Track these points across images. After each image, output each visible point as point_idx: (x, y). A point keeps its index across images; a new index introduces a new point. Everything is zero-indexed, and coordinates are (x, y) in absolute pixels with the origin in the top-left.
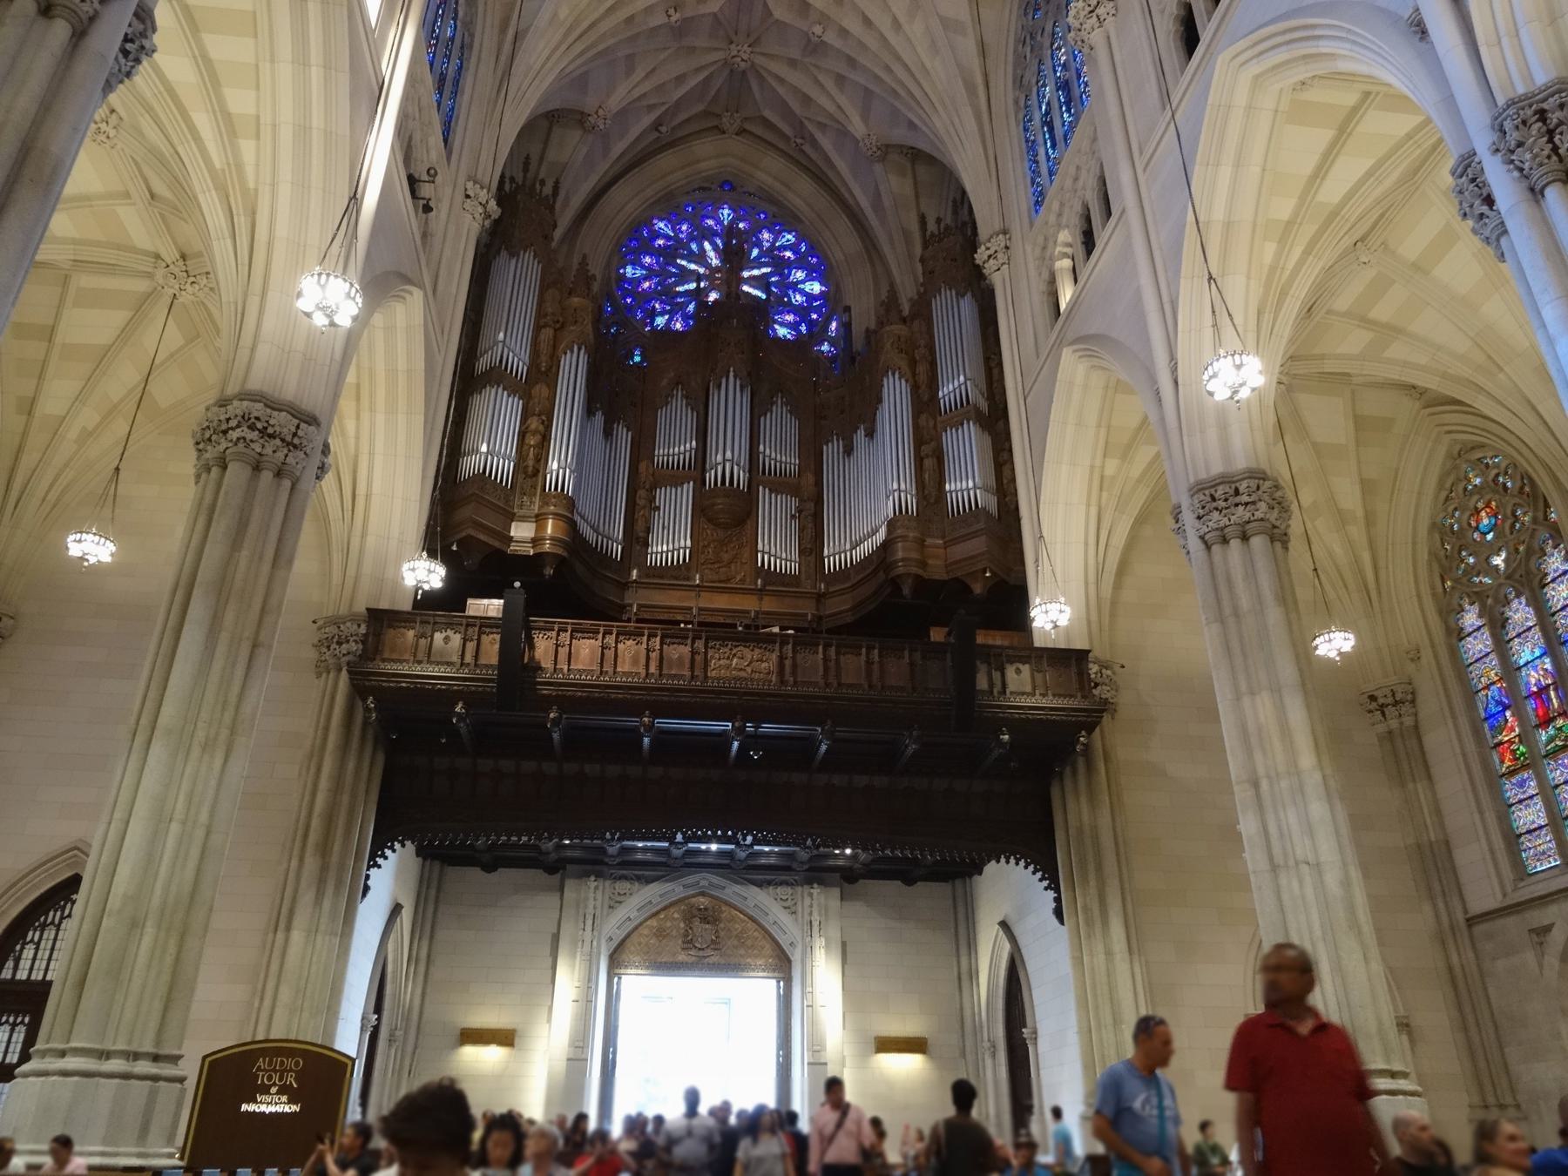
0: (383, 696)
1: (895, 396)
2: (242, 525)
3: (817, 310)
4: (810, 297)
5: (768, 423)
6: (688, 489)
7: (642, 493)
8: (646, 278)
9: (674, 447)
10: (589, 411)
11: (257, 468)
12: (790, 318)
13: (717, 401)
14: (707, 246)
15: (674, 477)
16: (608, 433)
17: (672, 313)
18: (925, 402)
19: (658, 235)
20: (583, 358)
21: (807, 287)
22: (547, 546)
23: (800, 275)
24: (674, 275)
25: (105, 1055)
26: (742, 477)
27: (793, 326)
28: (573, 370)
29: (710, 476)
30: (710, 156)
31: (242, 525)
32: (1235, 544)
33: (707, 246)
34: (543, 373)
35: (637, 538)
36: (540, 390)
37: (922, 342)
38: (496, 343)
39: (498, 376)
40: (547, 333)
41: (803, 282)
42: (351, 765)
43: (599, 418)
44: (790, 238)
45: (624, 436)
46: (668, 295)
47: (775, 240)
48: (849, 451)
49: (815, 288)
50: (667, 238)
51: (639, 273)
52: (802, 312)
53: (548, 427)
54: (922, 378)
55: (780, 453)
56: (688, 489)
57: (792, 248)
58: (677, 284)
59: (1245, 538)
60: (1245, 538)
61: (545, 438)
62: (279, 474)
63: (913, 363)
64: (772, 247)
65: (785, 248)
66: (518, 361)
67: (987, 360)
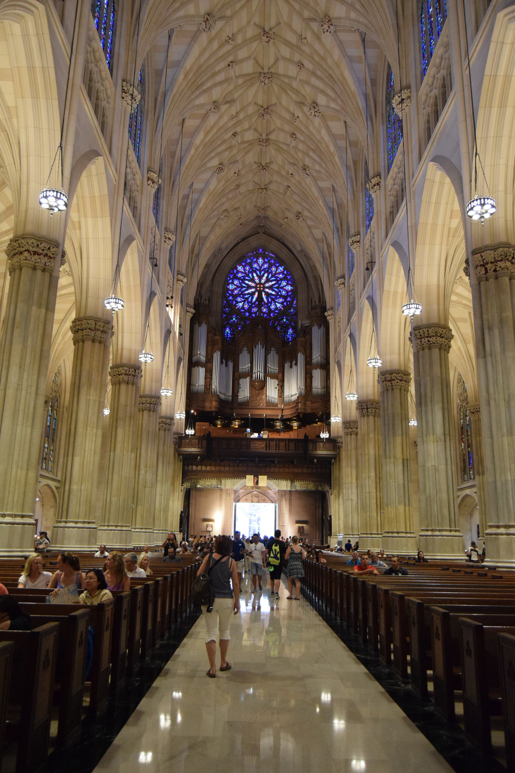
0: (183, 455)
1: (301, 357)
2: (164, 441)
3: (290, 296)
4: (287, 292)
5: (270, 357)
6: (248, 379)
7: (236, 382)
8: (235, 289)
9: (244, 366)
10: (222, 363)
11: (165, 430)
12: (281, 300)
13: (255, 351)
14: (255, 275)
15: (244, 375)
16: (226, 365)
17: (244, 301)
18: (308, 362)
19: (238, 272)
20: (219, 353)
21: (286, 288)
22: (213, 410)
23: (284, 283)
24: (245, 287)
25: (159, 530)
26: (262, 375)
27: (282, 303)
28: (217, 356)
29: (254, 376)
30: (254, 242)
31: (164, 441)
32: (349, 436)
33: (255, 275)
34: (209, 359)
35: (235, 394)
36: (209, 365)
37: (308, 343)
38: (197, 354)
39: (198, 364)
40: (210, 348)
41: (285, 286)
42: (176, 466)
43: (224, 361)
44: (281, 269)
45: (231, 364)
46: (242, 294)
47: (277, 270)
48: (291, 367)
49: (289, 288)
50: (242, 272)
51: (234, 287)
52: (285, 298)
53: (212, 376)
54: (308, 354)
55: (273, 367)
56: (248, 379)
57: (282, 273)
58: (247, 290)
59: (351, 434)
60: (351, 434)
61: (211, 378)
62: (168, 430)
63: (305, 351)
64: (276, 274)
65: (279, 273)
66: (203, 359)
67: (326, 347)
